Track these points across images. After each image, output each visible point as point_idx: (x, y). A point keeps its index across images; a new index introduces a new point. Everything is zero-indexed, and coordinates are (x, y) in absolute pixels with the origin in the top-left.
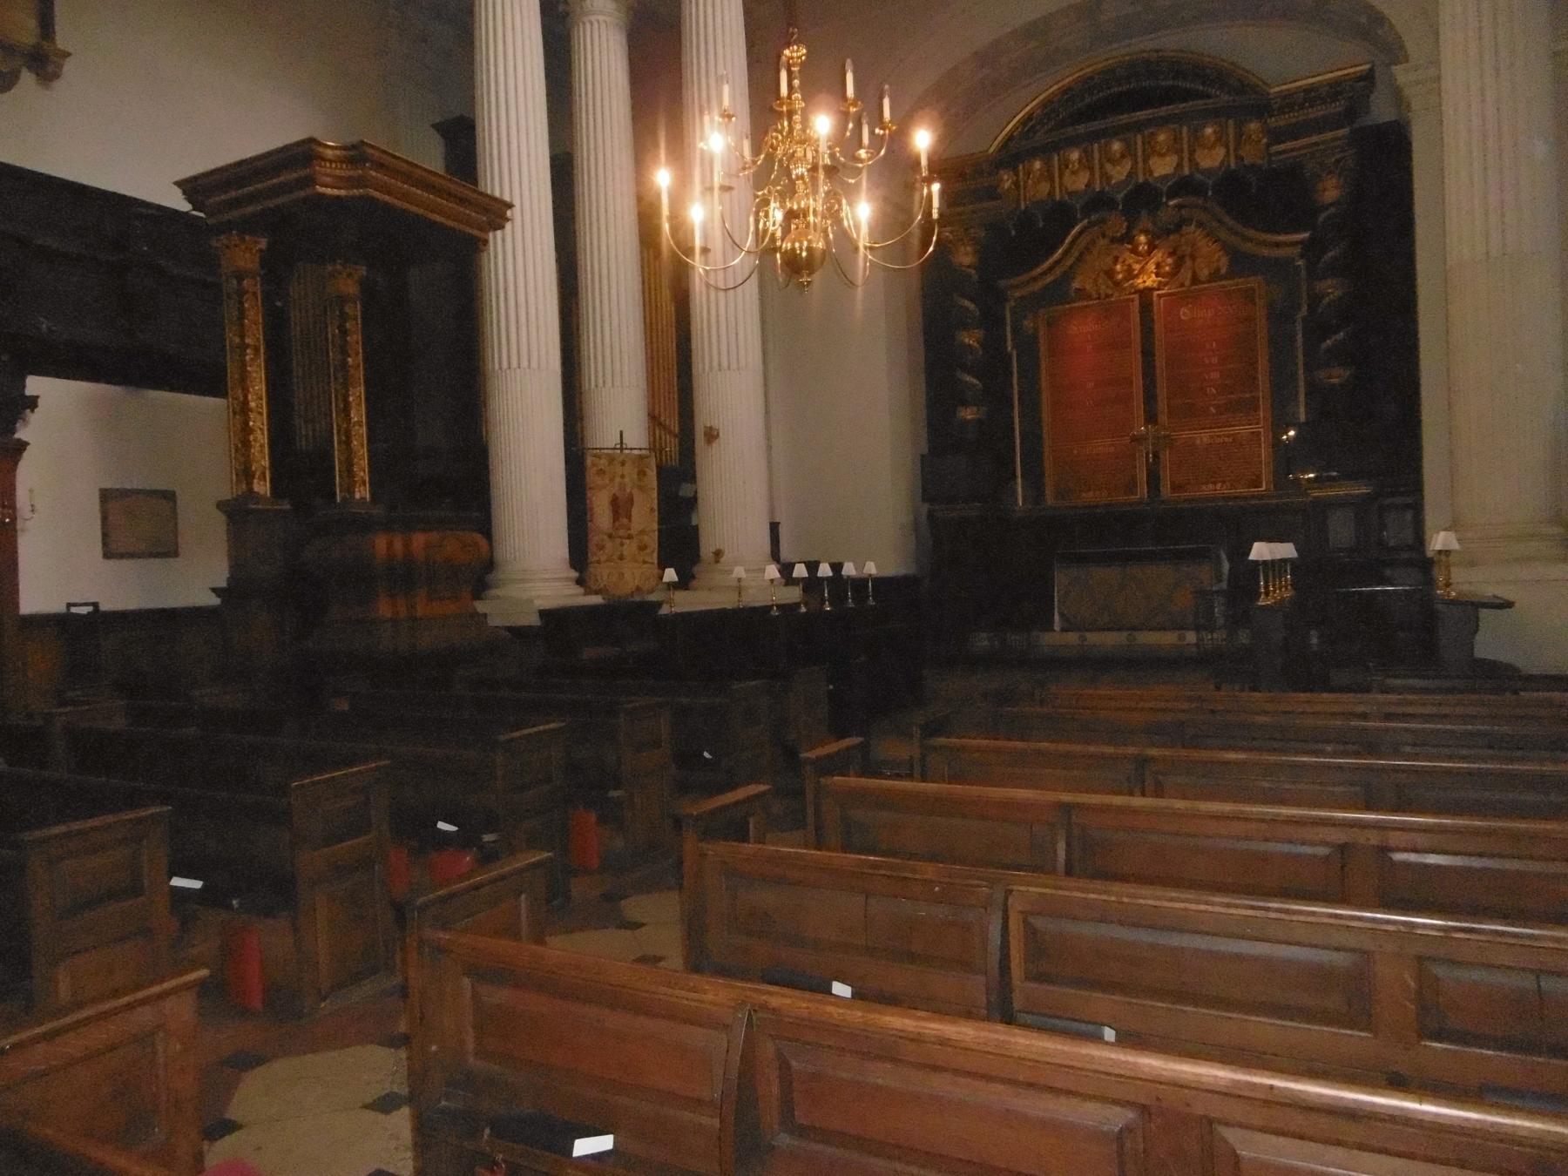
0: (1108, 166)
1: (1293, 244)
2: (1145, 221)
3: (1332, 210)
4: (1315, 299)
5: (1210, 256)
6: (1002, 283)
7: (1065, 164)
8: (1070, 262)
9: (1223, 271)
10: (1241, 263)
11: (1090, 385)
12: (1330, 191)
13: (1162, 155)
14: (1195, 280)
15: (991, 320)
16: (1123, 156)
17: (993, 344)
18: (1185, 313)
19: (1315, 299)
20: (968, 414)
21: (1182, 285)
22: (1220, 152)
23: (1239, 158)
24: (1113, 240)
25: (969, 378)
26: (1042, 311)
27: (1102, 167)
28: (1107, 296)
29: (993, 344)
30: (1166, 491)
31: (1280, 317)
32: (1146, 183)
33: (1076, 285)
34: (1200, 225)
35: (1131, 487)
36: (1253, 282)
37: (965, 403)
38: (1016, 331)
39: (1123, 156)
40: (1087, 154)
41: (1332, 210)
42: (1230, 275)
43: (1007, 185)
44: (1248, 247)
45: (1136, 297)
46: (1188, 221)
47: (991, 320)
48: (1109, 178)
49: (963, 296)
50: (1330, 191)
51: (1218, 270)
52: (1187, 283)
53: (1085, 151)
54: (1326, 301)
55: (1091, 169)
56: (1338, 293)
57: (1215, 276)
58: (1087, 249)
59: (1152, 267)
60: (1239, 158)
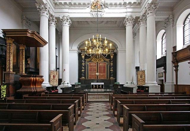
5: (102, 60)
10: (105, 61)
12: (112, 57)
17: (85, 64)
20: (83, 70)
29: (85, 64)
31: (107, 66)
35: (96, 78)
37: (83, 70)
49: (83, 60)
50: (112, 57)
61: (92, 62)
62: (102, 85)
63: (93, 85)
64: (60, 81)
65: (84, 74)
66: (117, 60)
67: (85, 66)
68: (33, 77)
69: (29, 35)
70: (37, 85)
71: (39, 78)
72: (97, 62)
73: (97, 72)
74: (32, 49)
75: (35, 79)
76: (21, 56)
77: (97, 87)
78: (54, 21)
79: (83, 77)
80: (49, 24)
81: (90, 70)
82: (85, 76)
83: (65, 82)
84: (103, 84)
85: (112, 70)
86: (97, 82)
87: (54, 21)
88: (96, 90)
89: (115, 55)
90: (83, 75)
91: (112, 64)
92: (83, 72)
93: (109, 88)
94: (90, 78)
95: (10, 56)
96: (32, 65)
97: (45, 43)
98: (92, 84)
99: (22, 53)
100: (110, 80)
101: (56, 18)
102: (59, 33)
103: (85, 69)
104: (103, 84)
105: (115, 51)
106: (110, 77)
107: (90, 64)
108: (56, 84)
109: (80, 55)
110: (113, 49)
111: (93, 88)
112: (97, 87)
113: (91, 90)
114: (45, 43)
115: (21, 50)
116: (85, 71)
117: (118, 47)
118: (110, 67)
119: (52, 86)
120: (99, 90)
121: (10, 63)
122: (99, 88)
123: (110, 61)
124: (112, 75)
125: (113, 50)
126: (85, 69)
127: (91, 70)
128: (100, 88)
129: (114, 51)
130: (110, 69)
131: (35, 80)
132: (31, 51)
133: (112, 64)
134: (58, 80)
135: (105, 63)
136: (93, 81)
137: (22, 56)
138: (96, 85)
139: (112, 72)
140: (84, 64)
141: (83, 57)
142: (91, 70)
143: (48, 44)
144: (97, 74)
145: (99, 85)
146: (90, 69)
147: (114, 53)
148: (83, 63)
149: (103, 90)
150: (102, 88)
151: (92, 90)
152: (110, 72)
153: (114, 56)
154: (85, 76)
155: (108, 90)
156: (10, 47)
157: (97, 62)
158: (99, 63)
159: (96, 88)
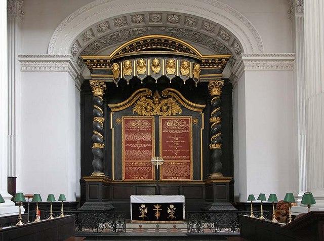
0: (153, 68)
1: (200, 108)
2: (157, 94)
4: (208, 124)
5: (176, 109)
6: (110, 105)
7: (138, 63)
12: (215, 92)
13: (171, 68)
14: (172, 114)
15: (107, 116)
16: (158, 65)
17: (107, 123)
18: (168, 124)
21: (168, 115)
22: (187, 71)
23: (193, 75)
24: (147, 98)
27: (150, 67)
28: (145, 115)
29: (107, 123)
30: (161, 179)
31: (196, 129)
32: (165, 76)
33: (134, 110)
34: (174, 98)
35: (150, 176)
39: (158, 65)
40: (145, 62)
42: (182, 115)
43: (116, 69)
44: (189, 107)
46: (170, 97)
47: (107, 116)
48: (153, 72)
49: (98, 105)
50: (215, 92)
53: (145, 61)
55: (147, 67)
56: (218, 122)
57: (177, 114)
58: (138, 99)
59: (159, 107)
60: (193, 75)
61: (136, 114)
62: (178, 206)
63: (137, 206)
65: (102, 160)
66: (234, 109)
67: (106, 131)
72: (157, 116)
73: (157, 155)
77: (157, 215)
79: (99, 174)
81: (126, 148)
82: (106, 169)
84: (180, 199)
85: (218, 146)
86: (158, 192)
89: (229, 88)
90: (97, 163)
91: (215, 120)
92: (99, 152)
94: (127, 176)
98: (134, 199)
100: (209, 186)
103: (107, 141)
104: (180, 199)
106: (209, 170)
107: (126, 121)
109: (85, 89)
111: (137, 216)
112: (157, 215)
113: (127, 225)
116: (107, 151)
118: (208, 133)
122: (164, 217)
124: (217, 165)
126: (107, 141)
127: (132, 145)
128: (170, 219)
129: (223, 67)
130: (208, 141)
133: (215, 120)
135: (187, 121)
136: (140, 189)
138: (150, 206)
139: (215, 155)
140: (100, 120)
141: (98, 92)
142: (132, 145)
144: (157, 161)
145: (165, 206)
146: (126, 143)
148: (98, 116)
150: (178, 216)
152: (209, 152)
154: (106, 169)
158: (164, 121)
159: (151, 217)
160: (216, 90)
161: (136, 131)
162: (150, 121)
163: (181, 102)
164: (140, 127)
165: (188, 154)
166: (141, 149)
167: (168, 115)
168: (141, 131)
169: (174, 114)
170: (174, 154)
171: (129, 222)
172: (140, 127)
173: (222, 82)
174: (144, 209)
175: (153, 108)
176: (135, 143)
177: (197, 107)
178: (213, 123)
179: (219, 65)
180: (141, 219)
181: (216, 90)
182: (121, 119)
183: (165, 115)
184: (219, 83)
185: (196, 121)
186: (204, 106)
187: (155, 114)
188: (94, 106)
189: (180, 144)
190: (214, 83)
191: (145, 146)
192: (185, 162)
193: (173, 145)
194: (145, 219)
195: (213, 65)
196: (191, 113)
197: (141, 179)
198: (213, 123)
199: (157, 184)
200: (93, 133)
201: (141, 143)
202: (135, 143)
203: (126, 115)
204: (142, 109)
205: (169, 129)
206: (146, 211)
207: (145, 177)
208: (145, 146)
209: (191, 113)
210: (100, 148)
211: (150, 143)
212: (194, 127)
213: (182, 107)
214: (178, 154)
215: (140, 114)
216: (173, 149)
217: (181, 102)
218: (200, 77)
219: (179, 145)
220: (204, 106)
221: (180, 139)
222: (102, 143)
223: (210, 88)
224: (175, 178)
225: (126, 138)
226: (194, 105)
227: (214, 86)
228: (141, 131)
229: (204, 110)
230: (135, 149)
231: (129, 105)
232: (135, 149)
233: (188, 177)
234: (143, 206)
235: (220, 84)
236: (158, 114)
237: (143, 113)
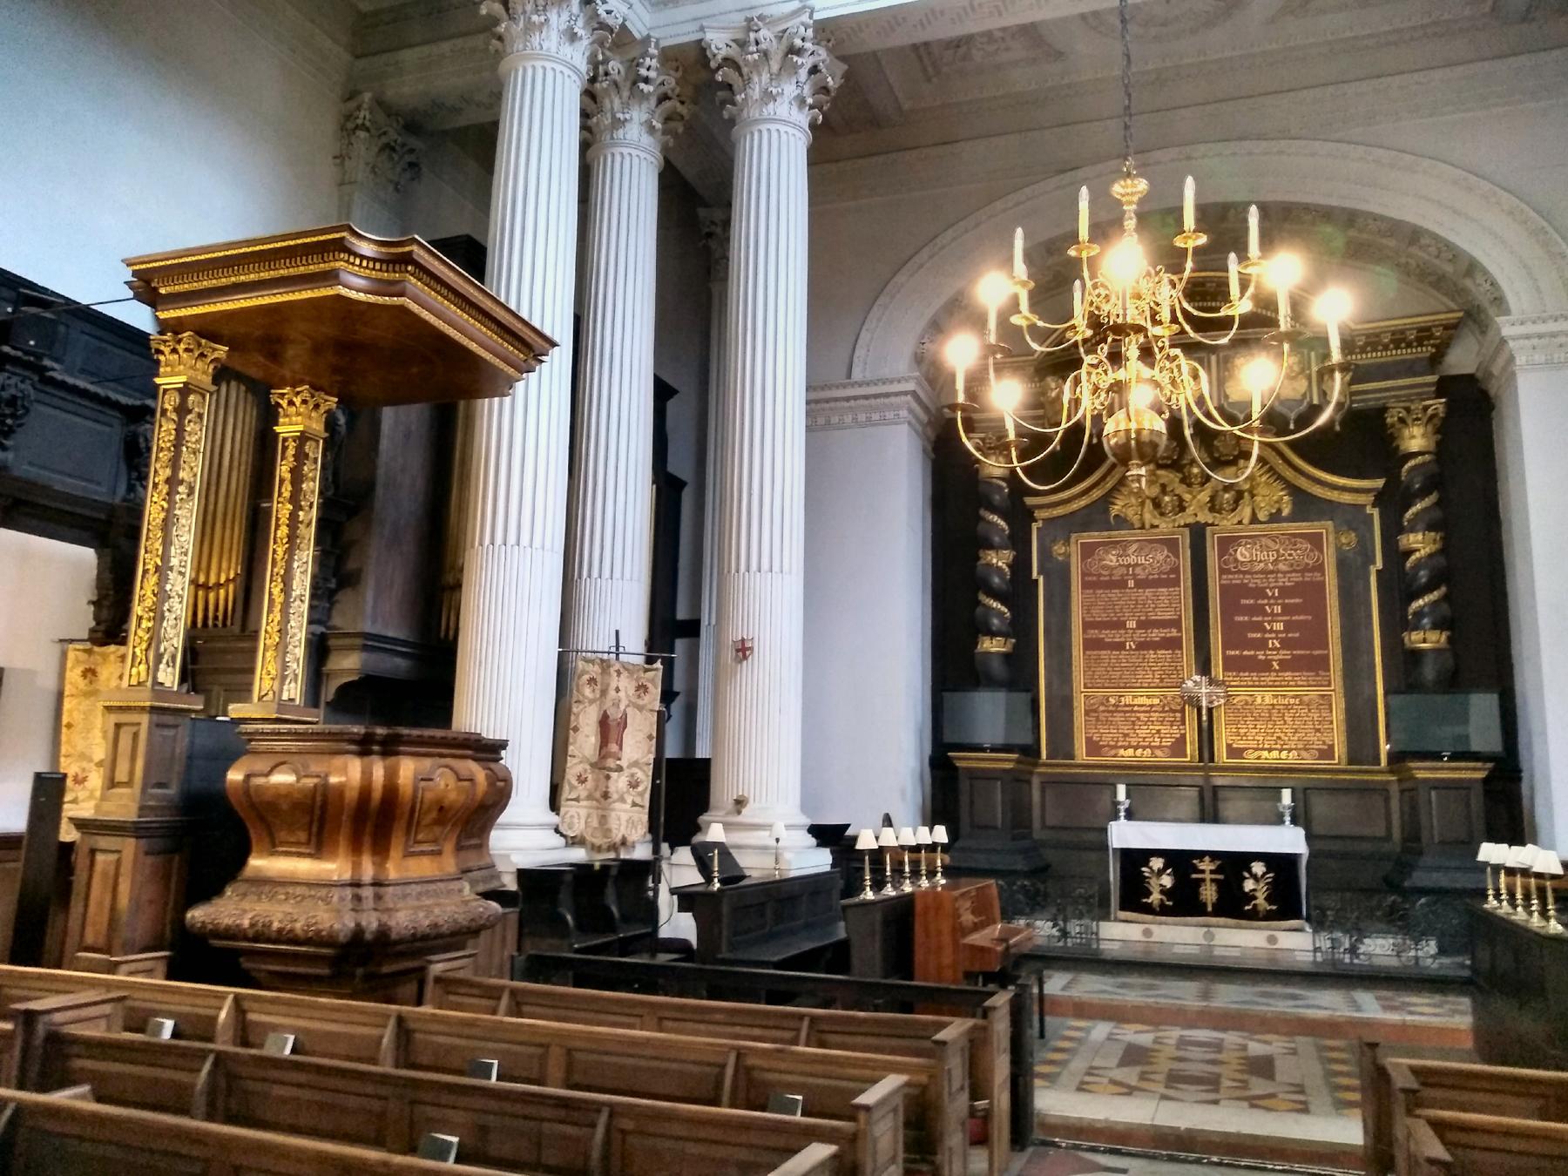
3: (1420, 459)
4: (1397, 557)
8: (1110, 484)
9: (1286, 512)
11: (1132, 624)
12: (1416, 440)
14: (1254, 519)
17: (1021, 565)
18: (1242, 554)
19: (1397, 557)
24: (1160, 467)
25: (995, 604)
26: (1074, 536)
28: (1153, 526)
29: (1021, 565)
30: (1222, 756)
33: (1115, 510)
36: (1324, 528)
38: (1045, 554)
41: (1420, 459)
42: (1293, 518)
44: (1318, 491)
45: (1187, 531)
49: (994, 510)
50: (1416, 440)
51: (1279, 511)
52: (1246, 521)
54: (1417, 555)
57: (1275, 517)
59: (1204, 496)
61: (1122, 522)
63: (1134, 859)
64: (683, 792)
67: (1019, 592)
68: (364, 747)
69: (354, 285)
70: (396, 852)
71: (427, 763)
74: (400, 428)
75: (379, 771)
76: (281, 509)
77: (1209, 894)
78: (644, 97)
80: (584, 127)
81: (1090, 645)
83: (740, 803)
86: (1209, 812)
87: (644, 97)
88: (1181, 937)
92: (997, 668)
93: (1398, 921)
94: (1094, 747)
95: (167, 524)
96: (378, 608)
97: (529, 346)
98: (1125, 834)
99: (297, 476)
101: (671, 57)
102: (702, 212)
103: (1022, 628)
104: (1289, 840)
105: (1461, 360)
107: (1088, 551)
108: (629, 825)
110: (1424, 334)
111: (1134, 899)
112: (1209, 894)
114: (529, 346)
115: (291, 451)
117: (1499, 301)
118: (1399, 586)
119: (578, 855)
120: (1240, 940)
121: (162, 595)
122: (1233, 906)
123: (1393, 501)
125: (1433, 342)
127: (1108, 636)
128: (1254, 915)
130: (1396, 622)
131: (377, 794)
132: (384, 444)
134: (646, 785)
135: (1316, 541)
136: (1150, 794)
137: (293, 517)
138: (1180, 861)
140: (999, 559)
142: (1108, 636)
143: (558, 362)
146: (1087, 626)
147: (1445, 386)
148: (991, 547)
149: (1296, 943)
150: (1285, 905)
151: (1121, 933)
153: (1444, 430)
155: (1379, 948)
156: (180, 431)
157: (1198, 533)
158: (1227, 544)
159: (1184, 903)
160: (1417, 431)
161: (1122, 584)
162: (1172, 545)
163: (1289, 474)
164: (1138, 570)
165: (1321, 664)
166: (1142, 646)
167: (1240, 523)
168: (1141, 584)
169: (1262, 516)
170: (1266, 666)
171: (1106, 917)
172: (1138, 570)
173: (1438, 405)
174: (1160, 872)
175: (1181, 500)
176: (1120, 625)
177: (1353, 490)
178: (1411, 552)
179: (1421, 345)
180: (1148, 909)
181: (1417, 431)
182: (1067, 542)
183: (1227, 524)
184: (1426, 408)
185: (1349, 539)
186: (1379, 483)
187: (1191, 520)
188: (982, 512)
189: (1289, 627)
190: (1408, 410)
191: (1156, 634)
192: (1313, 694)
193: (1264, 631)
194: (1164, 911)
195: (1397, 348)
196: (1325, 509)
197: (1144, 756)
198: (1411, 552)
199: (1207, 778)
200: (978, 603)
201: (1142, 625)
202: (1120, 625)
203: (1086, 526)
204: (1142, 504)
205: (1244, 573)
206: (1167, 881)
207: (1158, 752)
208: (1156, 634)
209: (1325, 509)
210: (998, 653)
211: (1176, 623)
212: (1342, 565)
213: (1294, 491)
214: (1285, 665)
215: (1137, 525)
216: (1262, 644)
217: (1289, 474)
218: (1353, 394)
219: (1286, 630)
220: (1379, 483)
221: (1287, 610)
222: (1006, 635)
223: (1393, 426)
224: (1275, 754)
225: (1087, 609)
226: (1342, 481)
227: (1409, 421)
228: (1141, 584)
229: (1380, 498)
230: (1120, 646)
231: (1096, 494)
232: (1120, 646)
233: (1327, 753)
234: (1157, 863)
235: (1430, 411)
236: (1202, 518)
237: (1147, 516)
